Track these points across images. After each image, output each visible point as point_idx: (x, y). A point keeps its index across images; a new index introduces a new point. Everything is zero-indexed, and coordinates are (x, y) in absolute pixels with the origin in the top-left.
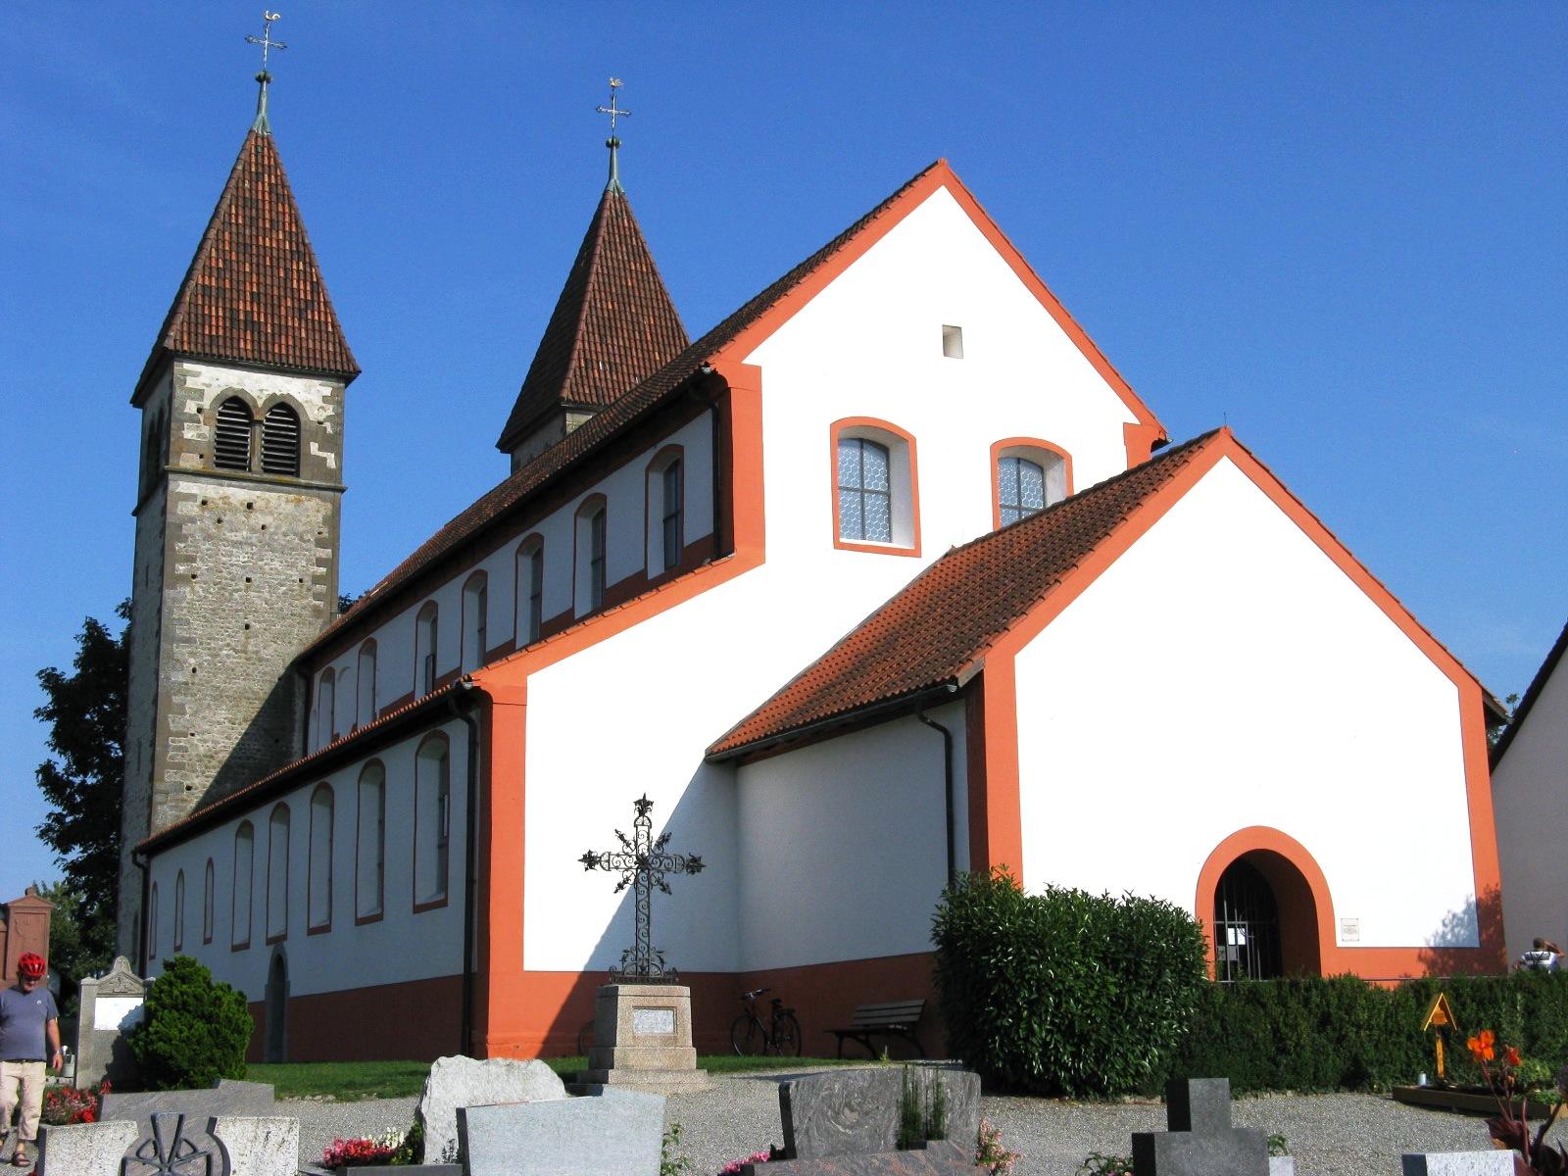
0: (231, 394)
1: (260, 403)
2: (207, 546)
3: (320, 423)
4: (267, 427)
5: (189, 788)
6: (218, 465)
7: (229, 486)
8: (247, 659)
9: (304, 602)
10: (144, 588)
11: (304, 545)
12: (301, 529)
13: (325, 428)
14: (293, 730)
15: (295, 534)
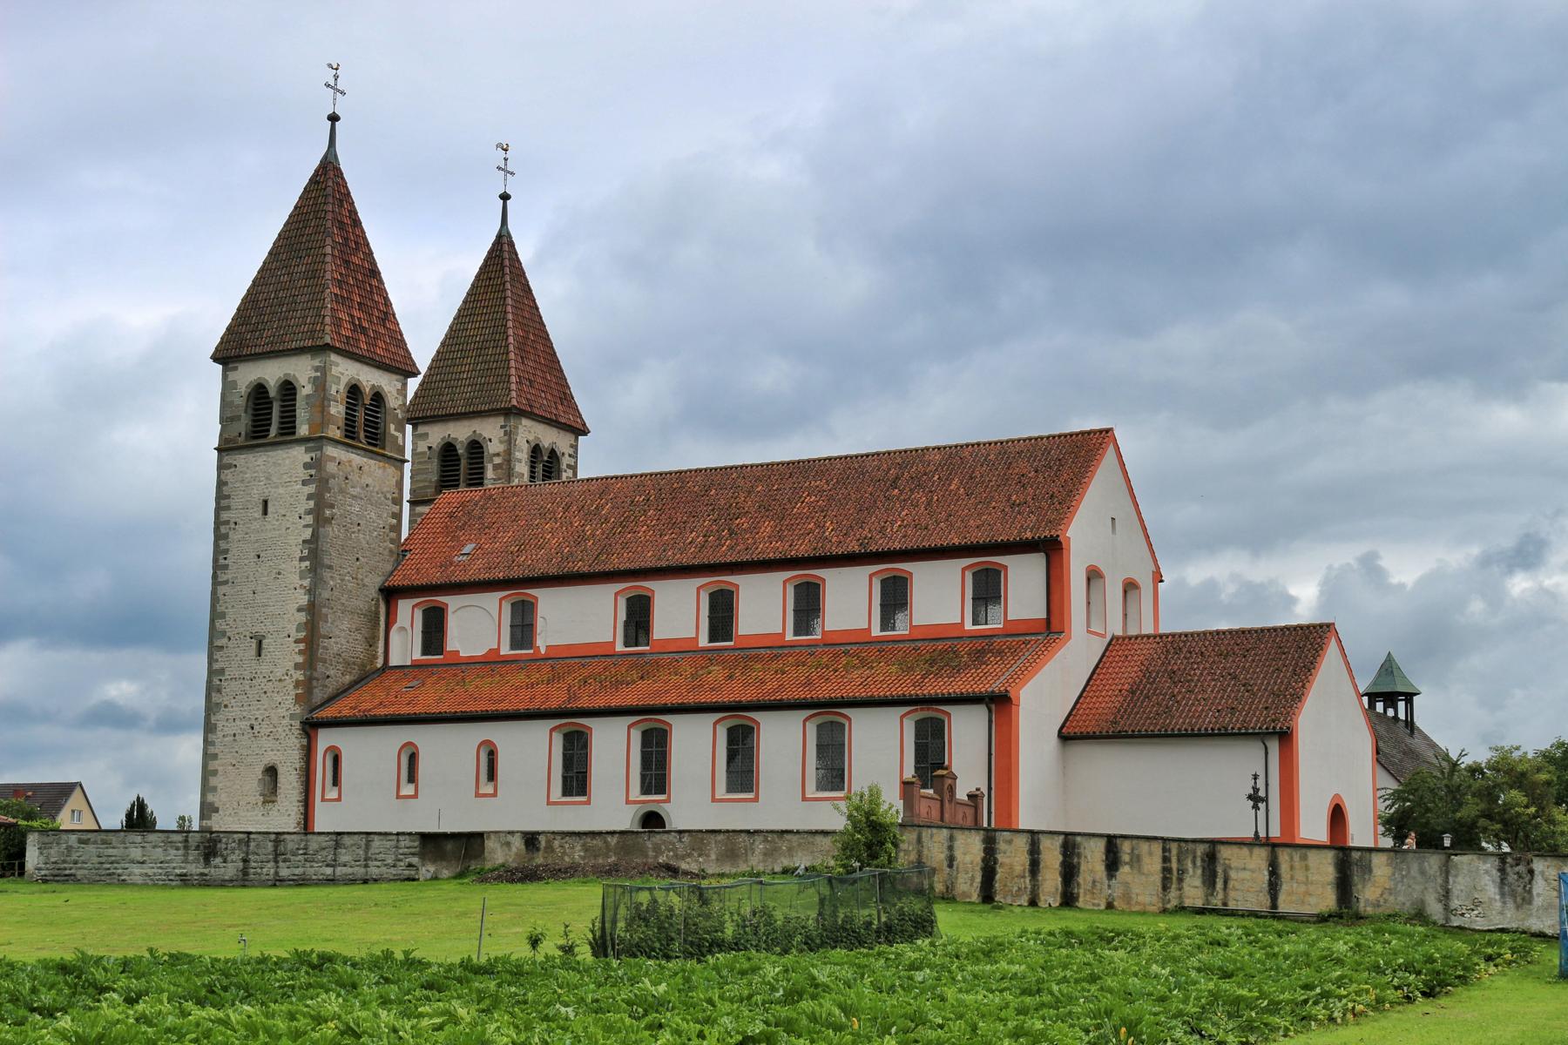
0: (354, 382)
1: (367, 390)
2: (340, 497)
4: (366, 409)
5: (328, 677)
6: (346, 436)
7: (352, 453)
8: (358, 584)
9: (385, 544)
10: (258, 513)
12: (385, 489)
14: (378, 640)
15: (382, 493)
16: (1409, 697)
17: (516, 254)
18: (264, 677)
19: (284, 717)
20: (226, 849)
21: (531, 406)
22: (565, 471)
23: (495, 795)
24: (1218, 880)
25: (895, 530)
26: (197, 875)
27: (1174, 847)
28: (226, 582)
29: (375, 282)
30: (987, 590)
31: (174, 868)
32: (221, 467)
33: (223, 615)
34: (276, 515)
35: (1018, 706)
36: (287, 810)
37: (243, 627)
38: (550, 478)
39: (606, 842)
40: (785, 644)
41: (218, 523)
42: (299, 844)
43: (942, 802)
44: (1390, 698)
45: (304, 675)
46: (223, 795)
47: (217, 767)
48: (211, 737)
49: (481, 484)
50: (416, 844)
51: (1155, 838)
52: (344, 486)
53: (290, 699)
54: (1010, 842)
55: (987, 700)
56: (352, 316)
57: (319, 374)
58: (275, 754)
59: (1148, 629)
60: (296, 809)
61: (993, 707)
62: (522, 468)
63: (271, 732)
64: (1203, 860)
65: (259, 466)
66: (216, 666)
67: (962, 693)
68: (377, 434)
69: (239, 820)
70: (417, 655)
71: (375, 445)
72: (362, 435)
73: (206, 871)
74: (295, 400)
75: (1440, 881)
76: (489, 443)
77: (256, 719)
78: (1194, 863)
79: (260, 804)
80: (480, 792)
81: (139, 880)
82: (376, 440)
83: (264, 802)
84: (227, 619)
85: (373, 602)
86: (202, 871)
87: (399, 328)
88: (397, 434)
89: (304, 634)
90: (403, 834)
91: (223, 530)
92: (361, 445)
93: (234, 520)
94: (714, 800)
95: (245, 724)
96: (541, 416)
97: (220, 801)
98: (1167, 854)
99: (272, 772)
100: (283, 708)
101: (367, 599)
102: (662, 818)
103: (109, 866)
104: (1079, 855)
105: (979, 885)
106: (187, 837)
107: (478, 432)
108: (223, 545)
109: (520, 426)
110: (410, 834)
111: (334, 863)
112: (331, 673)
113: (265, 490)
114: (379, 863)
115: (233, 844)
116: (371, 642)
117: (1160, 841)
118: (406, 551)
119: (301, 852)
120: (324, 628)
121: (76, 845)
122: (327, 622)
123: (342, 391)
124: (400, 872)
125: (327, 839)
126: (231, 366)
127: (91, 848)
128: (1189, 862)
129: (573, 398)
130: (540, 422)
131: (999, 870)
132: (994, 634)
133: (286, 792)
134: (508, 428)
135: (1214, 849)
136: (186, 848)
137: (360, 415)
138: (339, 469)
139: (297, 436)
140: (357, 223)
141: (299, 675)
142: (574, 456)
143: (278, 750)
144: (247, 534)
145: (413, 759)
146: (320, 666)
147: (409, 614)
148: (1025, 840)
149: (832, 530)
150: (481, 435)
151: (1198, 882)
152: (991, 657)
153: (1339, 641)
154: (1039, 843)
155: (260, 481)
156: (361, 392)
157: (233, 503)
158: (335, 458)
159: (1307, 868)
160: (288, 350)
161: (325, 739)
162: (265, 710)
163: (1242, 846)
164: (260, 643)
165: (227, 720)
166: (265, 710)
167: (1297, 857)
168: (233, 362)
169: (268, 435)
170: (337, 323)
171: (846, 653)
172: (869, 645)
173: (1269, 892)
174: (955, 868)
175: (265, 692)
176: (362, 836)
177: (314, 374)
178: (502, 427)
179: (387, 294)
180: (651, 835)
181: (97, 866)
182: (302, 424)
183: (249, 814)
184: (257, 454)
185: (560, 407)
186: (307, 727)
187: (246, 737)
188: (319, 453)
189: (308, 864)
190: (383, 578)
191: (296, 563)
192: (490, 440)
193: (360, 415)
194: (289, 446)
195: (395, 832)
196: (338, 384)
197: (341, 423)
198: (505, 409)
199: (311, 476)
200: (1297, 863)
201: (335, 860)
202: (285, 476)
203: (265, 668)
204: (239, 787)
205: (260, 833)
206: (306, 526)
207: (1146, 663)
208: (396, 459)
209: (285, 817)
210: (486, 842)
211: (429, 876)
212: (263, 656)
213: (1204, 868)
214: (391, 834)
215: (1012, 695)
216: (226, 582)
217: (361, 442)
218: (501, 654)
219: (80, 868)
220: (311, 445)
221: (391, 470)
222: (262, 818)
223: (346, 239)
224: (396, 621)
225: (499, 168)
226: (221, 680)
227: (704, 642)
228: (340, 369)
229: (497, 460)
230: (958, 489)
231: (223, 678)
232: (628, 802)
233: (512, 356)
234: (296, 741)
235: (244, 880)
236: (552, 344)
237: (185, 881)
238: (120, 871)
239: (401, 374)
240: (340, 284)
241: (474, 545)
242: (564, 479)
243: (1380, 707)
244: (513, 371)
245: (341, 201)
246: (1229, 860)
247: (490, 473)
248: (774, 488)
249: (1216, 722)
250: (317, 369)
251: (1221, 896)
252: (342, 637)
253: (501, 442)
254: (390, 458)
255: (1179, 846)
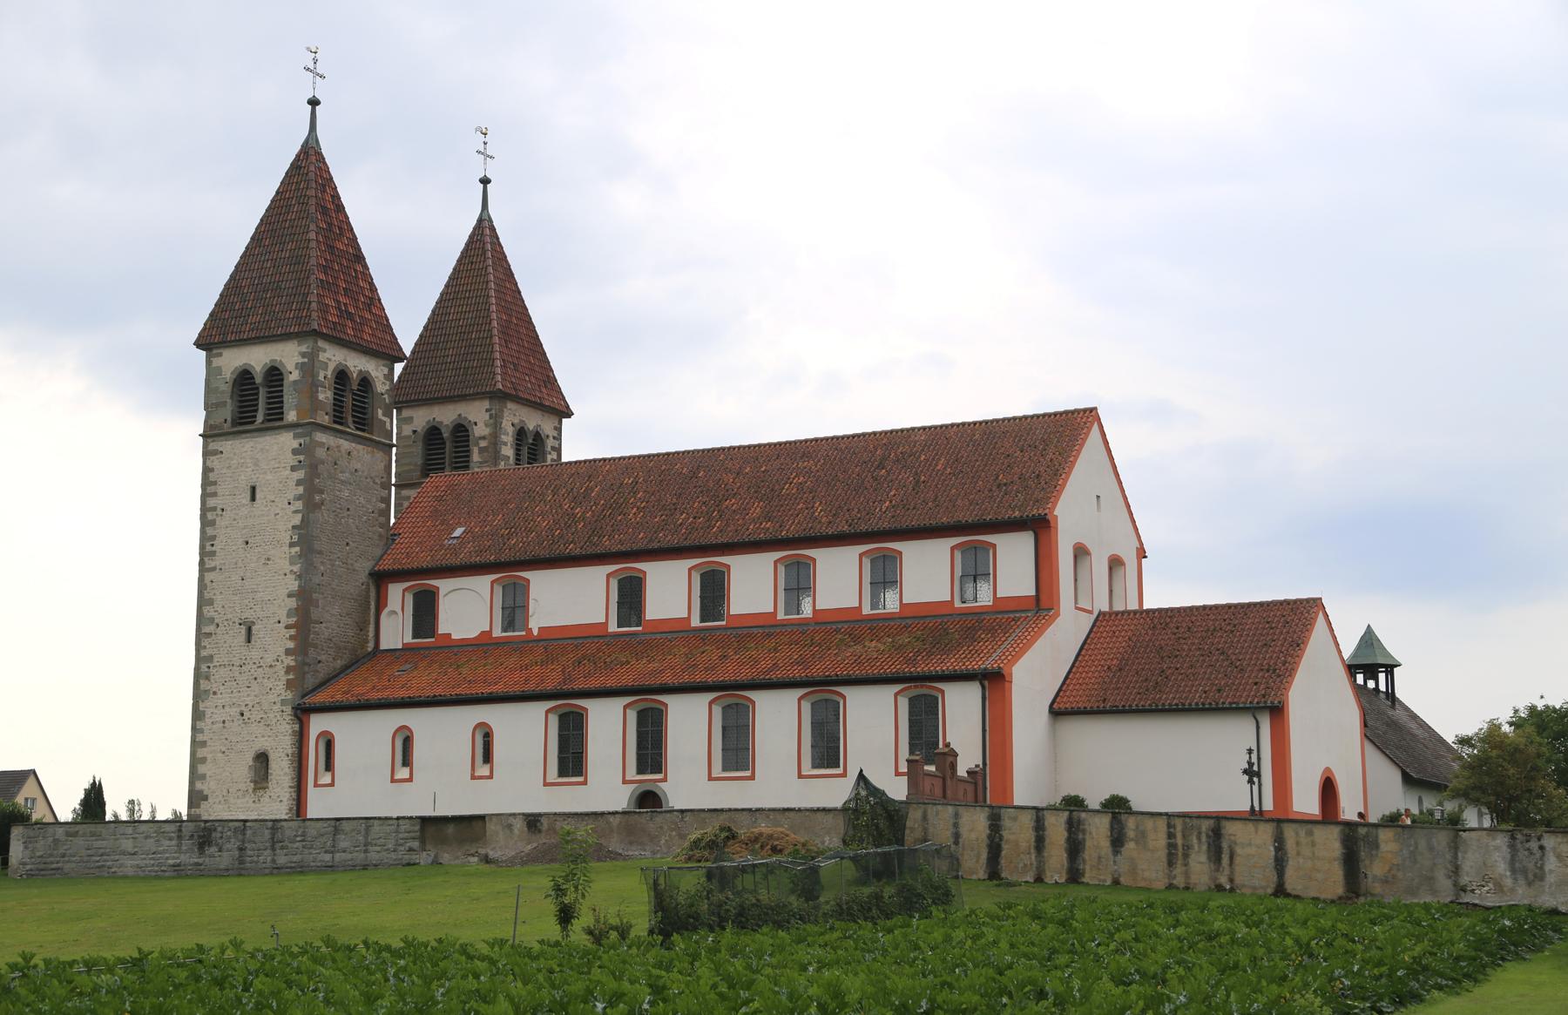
0: (341, 368)
1: (355, 375)
2: (329, 483)
3: (382, 394)
5: (319, 662)
6: (335, 422)
7: (342, 438)
8: (348, 569)
11: (375, 486)
12: (373, 475)
13: (385, 399)
14: (369, 624)
15: (371, 478)
16: (1390, 669)
17: (498, 239)
18: (254, 663)
19: (274, 703)
20: (222, 837)
21: (515, 390)
22: (550, 453)
23: (491, 777)
24: (1223, 856)
25: (883, 510)
26: (191, 865)
27: (1178, 823)
28: (214, 569)
29: (359, 268)
30: (976, 568)
31: (167, 858)
32: (206, 454)
33: (211, 602)
34: (264, 501)
35: (1011, 682)
36: (278, 797)
37: (231, 613)
38: (535, 460)
39: (608, 823)
40: (778, 623)
41: (205, 510)
42: (297, 831)
43: (944, 779)
44: (1371, 671)
45: (296, 660)
46: (212, 783)
47: (205, 755)
48: (200, 725)
49: (467, 467)
50: (417, 828)
51: (1160, 814)
52: (333, 471)
53: (281, 685)
54: (1015, 819)
55: (980, 677)
56: (339, 302)
57: (306, 360)
58: (267, 740)
59: (1133, 605)
60: (288, 795)
61: (986, 683)
62: (508, 451)
63: (262, 718)
64: (1208, 836)
65: (246, 452)
66: (204, 653)
67: (956, 671)
68: (365, 419)
69: (229, 807)
70: (409, 639)
71: (363, 430)
72: (350, 420)
73: (200, 861)
74: (282, 385)
75: (1448, 857)
76: (474, 427)
77: (246, 705)
78: (1199, 839)
79: (251, 791)
80: (476, 774)
81: (130, 872)
82: (364, 425)
83: (254, 790)
84: (215, 605)
85: (364, 587)
86: (196, 860)
87: (385, 314)
88: (384, 419)
89: (295, 619)
90: (404, 818)
91: (210, 516)
92: (348, 430)
93: (220, 507)
94: (710, 778)
95: (235, 711)
96: (527, 400)
97: (209, 789)
98: (1172, 830)
99: (262, 759)
100: (275, 692)
101: (357, 584)
102: (660, 799)
103: (98, 858)
104: (1084, 831)
105: (985, 862)
106: (180, 826)
107: (463, 416)
108: (210, 531)
109: (505, 410)
110: (411, 818)
111: (333, 849)
112: (323, 658)
113: (253, 476)
114: (378, 848)
115: (229, 833)
116: (362, 627)
117: (1165, 817)
118: (395, 535)
119: (298, 839)
120: (315, 614)
121: (63, 838)
122: (318, 607)
123: (329, 376)
124: (400, 857)
125: (325, 825)
126: (215, 351)
127: (79, 841)
128: (1194, 838)
129: (556, 381)
130: (523, 404)
131: (1005, 846)
132: (984, 611)
133: (277, 778)
134: (493, 412)
135: (1219, 824)
136: (180, 837)
137: (348, 401)
138: (328, 455)
139: (285, 422)
140: (340, 208)
141: (290, 661)
142: (558, 438)
143: (269, 736)
144: (235, 520)
145: (408, 743)
146: (311, 651)
147: (398, 596)
148: (1029, 817)
149: (821, 510)
150: (466, 418)
151: (1203, 858)
152: (981, 634)
153: (1326, 616)
154: (1044, 819)
155: (247, 467)
156: (349, 378)
157: (219, 489)
158: (324, 444)
159: (1313, 844)
160: (274, 336)
161: (318, 724)
162: (255, 696)
163: (1247, 822)
164: (249, 630)
165: (216, 707)
166: (255, 696)
167: (1302, 833)
168: (217, 348)
169: (255, 421)
170: (324, 309)
171: (837, 631)
172: (859, 623)
173: (1275, 867)
174: (961, 843)
175: (255, 679)
176: (361, 821)
177: (301, 360)
178: (487, 410)
179: (372, 279)
180: (654, 814)
181: (86, 859)
182: (289, 410)
183: (239, 801)
184: (243, 440)
185: (544, 390)
186: (299, 712)
187: (236, 723)
188: (308, 438)
189: (306, 851)
190: (373, 563)
191: (286, 549)
192: (476, 424)
193: (348, 401)
194: (277, 432)
195: (395, 816)
196: (326, 369)
197: (330, 408)
198: (490, 392)
199: (300, 462)
200: (1304, 839)
201: (334, 846)
202: (273, 462)
203: (255, 654)
204: (228, 774)
205: (256, 821)
206: (296, 512)
207: (1134, 639)
208: (384, 444)
209: (276, 804)
210: (488, 825)
211: (430, 860)
212: (253, 642)
213: (1209, 844)
214: (391, 818)
215: (1005, 672)
216: (214, 569)
217: (349, 427)
218: (494, 636)
219: (68, 862)
220: (299, 430)
221: (379, 455)
222: (253, 805)
223: (330, 225)
224: (386, 605)
225: (478, 152)
226: (209, 667)
227: (696, 622)
228: (327, 355)
229: (483, 444)
230: (945, 468)
231: (211, 665)
232: (625, 782)
233: (496, 340)
234: (288, 727)
235: (240, 869)
236: (534, 327)
237: (178, 872)
238: (108, 863)
239: (388, 360)
240: (325, 269)
241: (463, 529)
242: (549, 462)
243: (1360, 679)
244: (497, 355)
245: (324, 186)
246: (1234, 835)
247: (476, 457)
248: (763, 469)
249: (1207, 697)
250: (303, 355)
251: (1227, 872)
252: (333, 621)
253: (486, 425)
254: (379, 442)
255: (1184, 821)
